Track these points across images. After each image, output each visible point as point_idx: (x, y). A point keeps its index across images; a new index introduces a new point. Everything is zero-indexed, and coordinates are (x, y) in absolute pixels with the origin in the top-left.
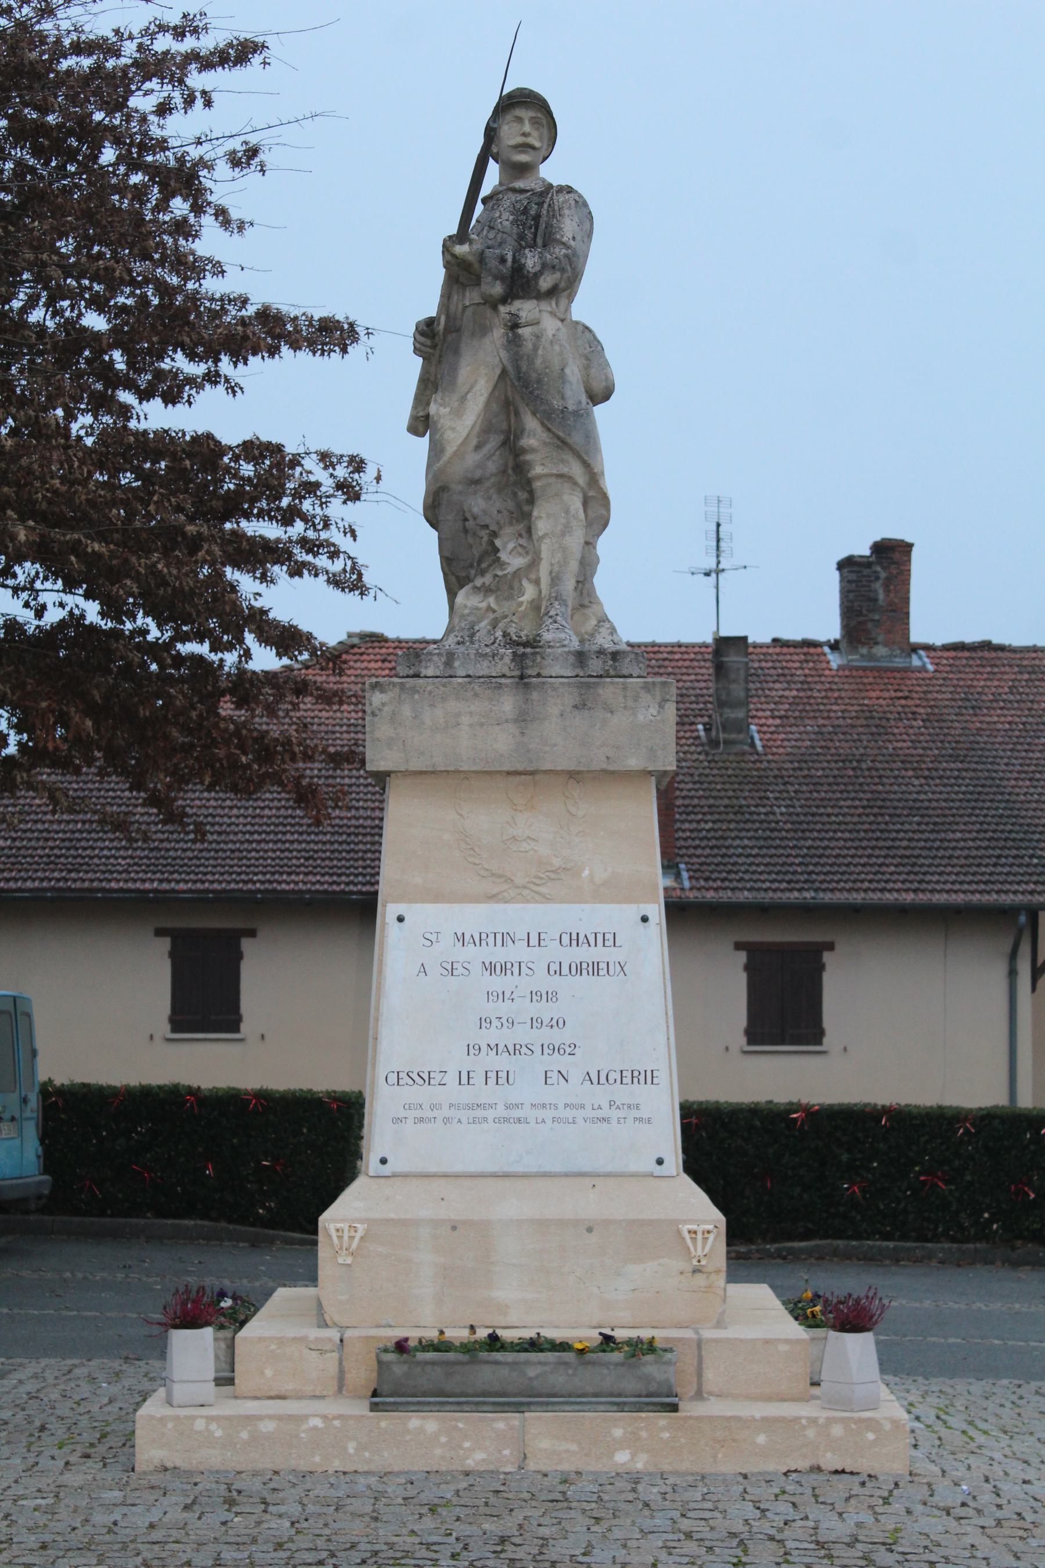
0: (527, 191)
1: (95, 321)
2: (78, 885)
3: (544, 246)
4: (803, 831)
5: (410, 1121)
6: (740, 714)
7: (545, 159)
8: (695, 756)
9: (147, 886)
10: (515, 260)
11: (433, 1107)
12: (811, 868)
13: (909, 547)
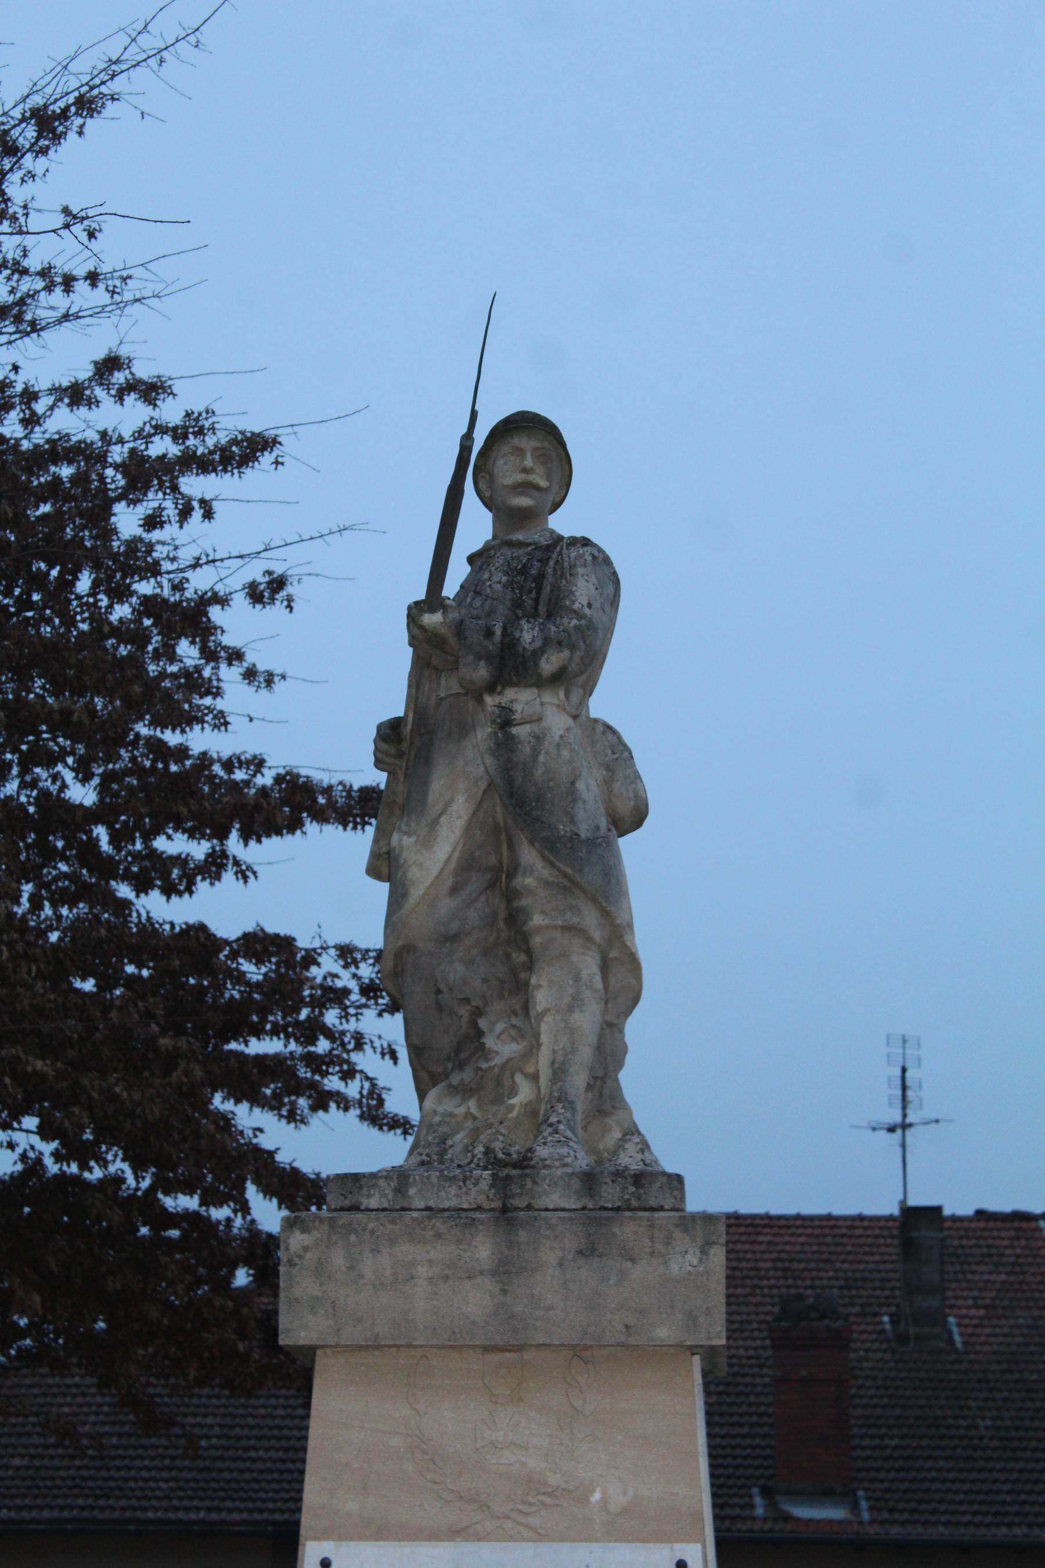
0: (529, 544)
3: (549, 616)
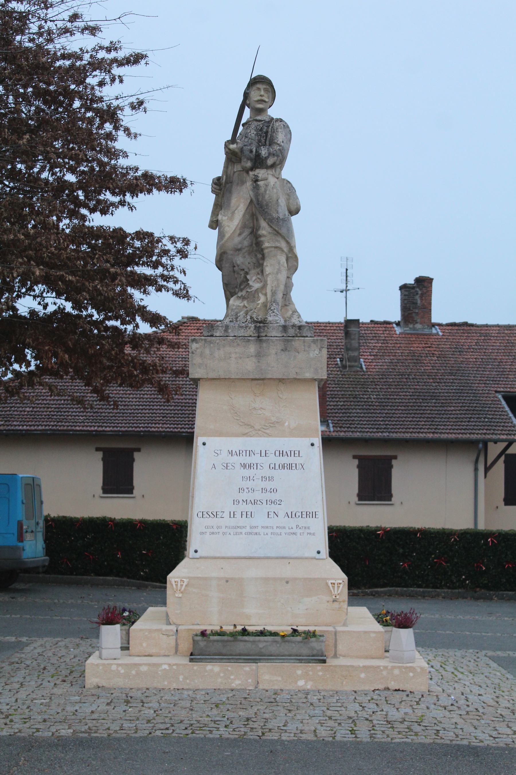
1: (70, 178)
2: (62, 428)
3: (270, 145)
4: (384, 406)
5: (208, 534)
6: (356, 354)
7: (270, 107)
8: (336, 372)
9: (92, 428)
10: (256, 151)
11: (218, 527)
12: (387, 422)
13: (432, 279)
